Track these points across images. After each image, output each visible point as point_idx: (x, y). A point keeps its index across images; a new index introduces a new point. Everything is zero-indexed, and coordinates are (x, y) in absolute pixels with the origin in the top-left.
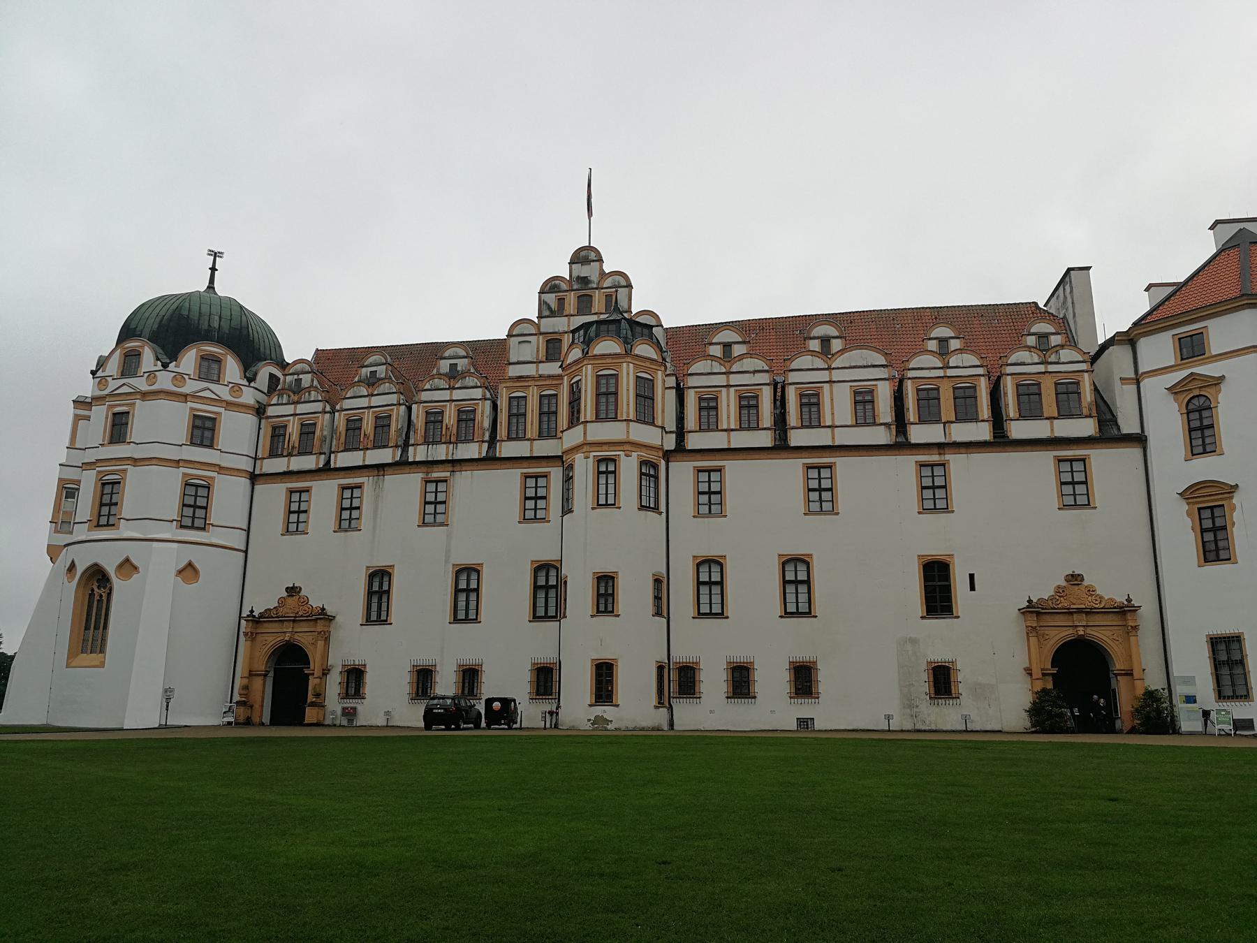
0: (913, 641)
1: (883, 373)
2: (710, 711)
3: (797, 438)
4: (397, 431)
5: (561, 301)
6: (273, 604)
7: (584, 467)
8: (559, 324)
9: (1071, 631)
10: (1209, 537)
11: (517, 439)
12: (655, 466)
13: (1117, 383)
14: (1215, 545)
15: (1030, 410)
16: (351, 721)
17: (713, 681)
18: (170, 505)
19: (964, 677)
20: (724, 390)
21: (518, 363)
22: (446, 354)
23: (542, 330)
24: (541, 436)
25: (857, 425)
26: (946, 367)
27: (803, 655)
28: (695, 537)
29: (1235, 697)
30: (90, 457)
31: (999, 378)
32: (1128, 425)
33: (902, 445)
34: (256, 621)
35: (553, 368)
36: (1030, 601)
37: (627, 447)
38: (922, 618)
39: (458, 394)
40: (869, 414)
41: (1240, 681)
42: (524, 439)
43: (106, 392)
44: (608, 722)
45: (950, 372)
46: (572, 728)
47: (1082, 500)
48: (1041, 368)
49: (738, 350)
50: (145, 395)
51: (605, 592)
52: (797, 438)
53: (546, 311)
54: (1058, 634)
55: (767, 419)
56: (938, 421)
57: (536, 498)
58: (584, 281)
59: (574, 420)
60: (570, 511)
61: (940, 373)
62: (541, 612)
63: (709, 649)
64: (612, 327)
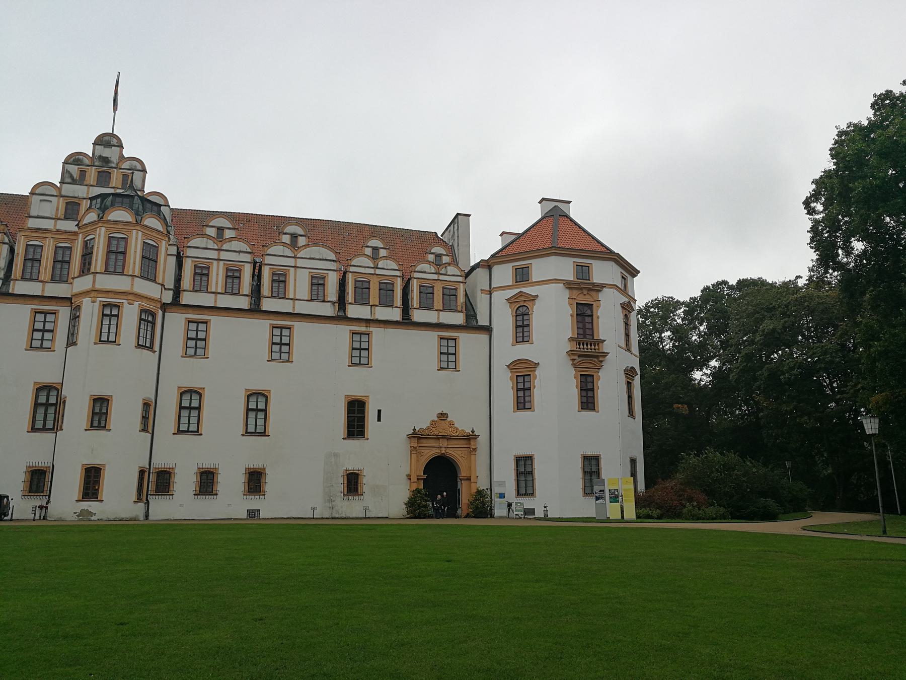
0: (336, 455)
1: (333, 266)
2: (181, 505)
3: (268, 304)
5: (83, 173)
7: (90, 310)
8: (80, 191)
9: (437, 450)
10: (521, 394)
11: (31, 279)
12: (154, 315)
13: (479, 292)
14: (523, 402)
17: (185, 482)
19: (367, 482)
20: (215, 262)
21: (38, 217)
23: (63, 193)
24: (53, 280)
25: (312, 300)
27: (256, 464)
28: (180, 371)
29: (526, 494)
31: (409, 280)
32: (483, 321)
33: (341, 318)
35: (70, 226)
36: (414, 430)
37: (131, 297)
38: (344, 439)
40: (321, 293)
41: (529, 484)
42: (37, 280)
44: (91, 514)
45: (378, 272)
46: (60, 520)
47: (452, 365)
48: (435, 277)
49: (228, 234)
51: (100, 412)
52: (268, 304)
53: (67, 177)
54: (429, 453)
55: (246, 288)
56: (368, 304)
58: (105, 160)
59: (85, 269)
61: (372, 271)
62: (39, 425)
63: (183, 457)
64: (126, 200)
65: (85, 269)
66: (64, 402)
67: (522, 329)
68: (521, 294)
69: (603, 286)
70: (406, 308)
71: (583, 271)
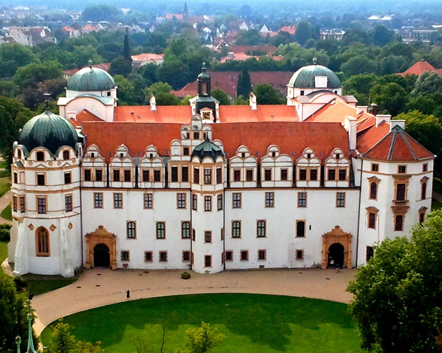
4: (133, 176)
5: (188, 134)
6: (94, 231)
14: (372, 224)
15: (332, 177)
16: (125, 267)
17: (237, 256)
18: (62, 205)
19: (306, 254)
21: (175, 155)
22: (148, 150)
23: (183, 144)
26: (309, 163)
28: (232, 214)
30: (28, 188)
32: (357, 184)
33: (294, 187)
35: (188, 158)
39: (154, 165)
43: (32, 166)
47: (342, 205)
50: (48, 169)
51: (208, 237)
52: (265, 184)
54: (332, 242)
57: (182, 201)
59: (197, 181)
60: (196, 210)
61: (307, 165)
63: (235, 246)
65: (197, 181)
66: (194, 231)
67: (373, 194)
69: (410, 176)
71: (402, 169)
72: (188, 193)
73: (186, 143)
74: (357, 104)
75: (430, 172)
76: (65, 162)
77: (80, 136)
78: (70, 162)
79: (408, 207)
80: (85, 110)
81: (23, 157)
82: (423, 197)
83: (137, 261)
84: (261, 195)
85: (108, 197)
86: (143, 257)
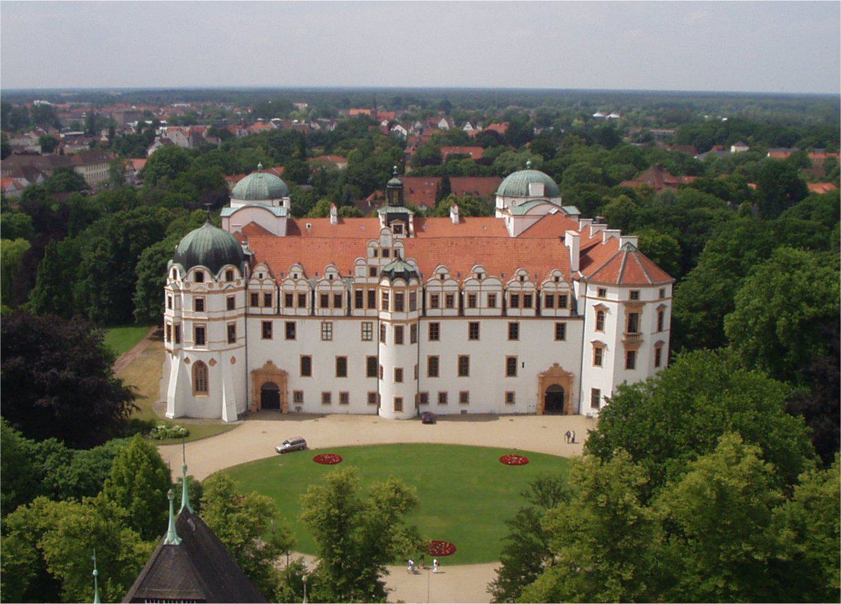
14: (598, 361)
15: (549, 304)
17: (433, 398)
32: (580, 313)
33: (504, 315)
34: (255, 373)
35: (375, 280)
49: (447, 277)
52: (468, 312)
54: (549, 383)
63: (432, 387)
65: (385, 306)
66: (382, 368)
67: (600, 326)
68: (600, 305)
69: (644, 303)
70: (538, 311)
71: (635, 295)
72: (375, 322)
73: (374, 262)
74: (580, 217)
75: (668, 298)
76: (229, 284)
77: (245, 252)
78: (234, 284)
79: (642, 341)
80: (253, 222)
81: (179, 278)
82: (660, 329)
83: (312, 402)
84: (464, 325)
85: (279, 327)
86: (319, 398)
